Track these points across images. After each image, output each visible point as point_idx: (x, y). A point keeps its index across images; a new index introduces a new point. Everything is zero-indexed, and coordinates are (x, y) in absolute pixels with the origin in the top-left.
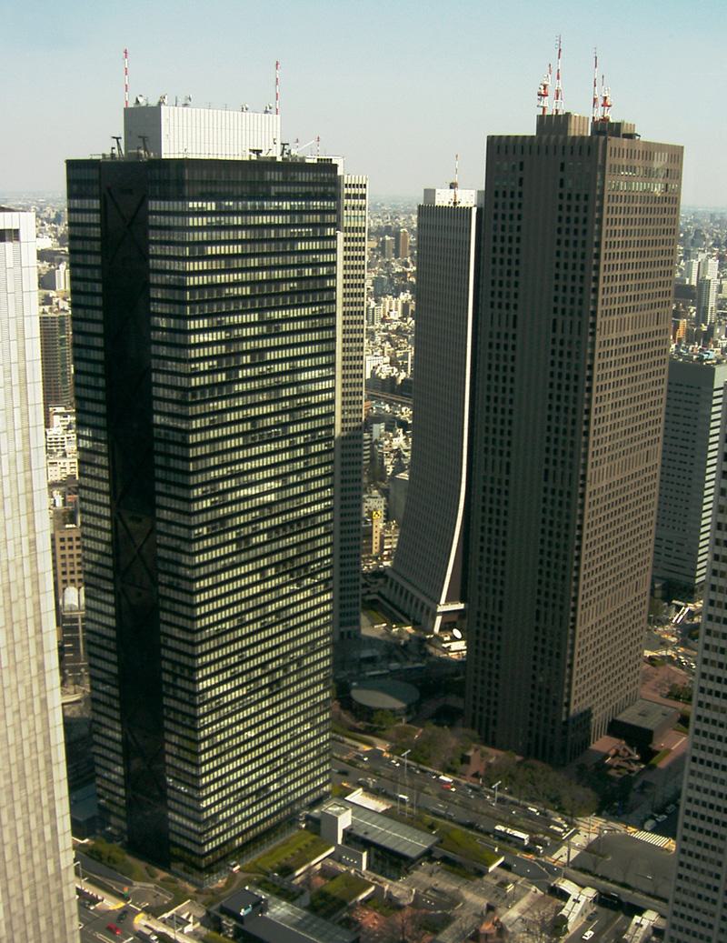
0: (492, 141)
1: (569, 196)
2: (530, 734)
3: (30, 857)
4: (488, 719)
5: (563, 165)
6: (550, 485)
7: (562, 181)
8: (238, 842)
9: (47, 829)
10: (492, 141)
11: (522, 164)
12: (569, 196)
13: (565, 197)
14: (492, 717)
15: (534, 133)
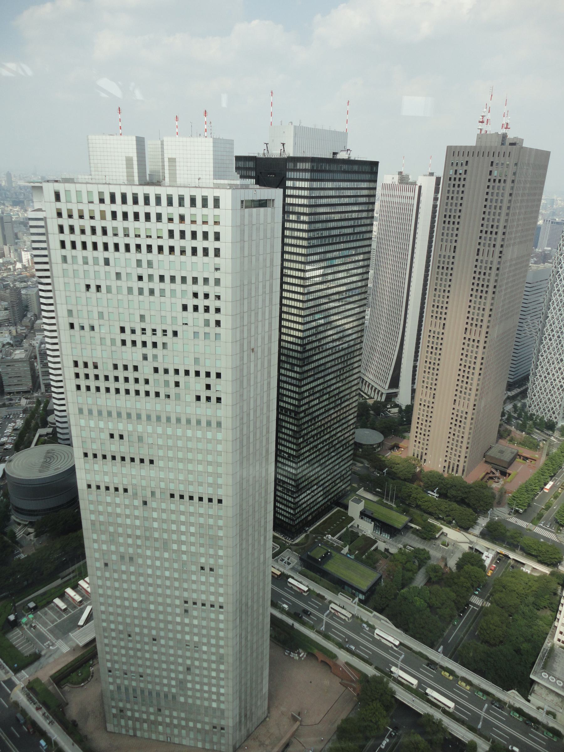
0: (449, 148)
1: (495, 180)
2: (446, 461)
3: (253, 554)
4: (422, 453)
5: (492, 162)
6: (468, 336)
7: (491, 172)
8: (310, 518)
9: (262, 538)
10: (449, 148)
11: (467, 162)
12: (495, 180)
13: (492, 181)
14: (425, 451)
15: (474, 144)
